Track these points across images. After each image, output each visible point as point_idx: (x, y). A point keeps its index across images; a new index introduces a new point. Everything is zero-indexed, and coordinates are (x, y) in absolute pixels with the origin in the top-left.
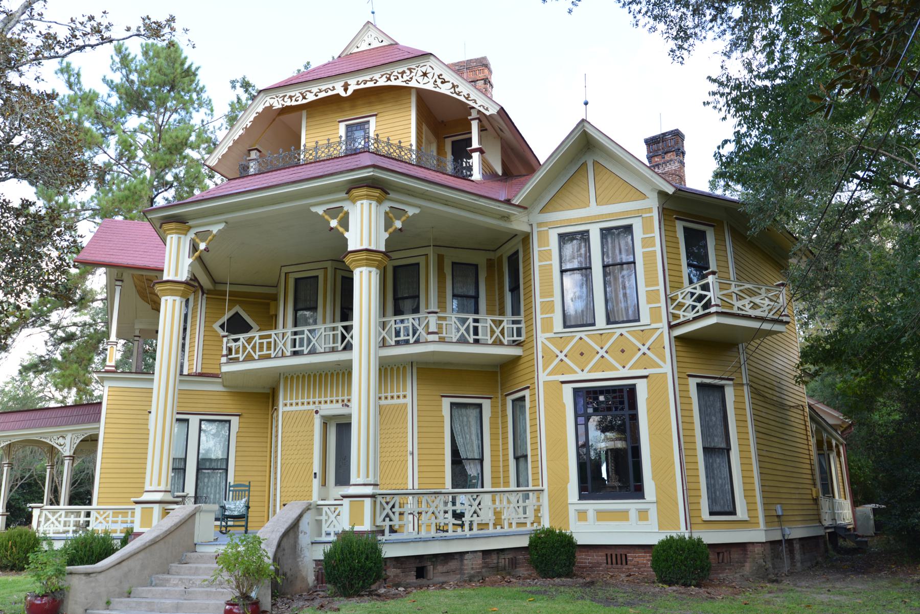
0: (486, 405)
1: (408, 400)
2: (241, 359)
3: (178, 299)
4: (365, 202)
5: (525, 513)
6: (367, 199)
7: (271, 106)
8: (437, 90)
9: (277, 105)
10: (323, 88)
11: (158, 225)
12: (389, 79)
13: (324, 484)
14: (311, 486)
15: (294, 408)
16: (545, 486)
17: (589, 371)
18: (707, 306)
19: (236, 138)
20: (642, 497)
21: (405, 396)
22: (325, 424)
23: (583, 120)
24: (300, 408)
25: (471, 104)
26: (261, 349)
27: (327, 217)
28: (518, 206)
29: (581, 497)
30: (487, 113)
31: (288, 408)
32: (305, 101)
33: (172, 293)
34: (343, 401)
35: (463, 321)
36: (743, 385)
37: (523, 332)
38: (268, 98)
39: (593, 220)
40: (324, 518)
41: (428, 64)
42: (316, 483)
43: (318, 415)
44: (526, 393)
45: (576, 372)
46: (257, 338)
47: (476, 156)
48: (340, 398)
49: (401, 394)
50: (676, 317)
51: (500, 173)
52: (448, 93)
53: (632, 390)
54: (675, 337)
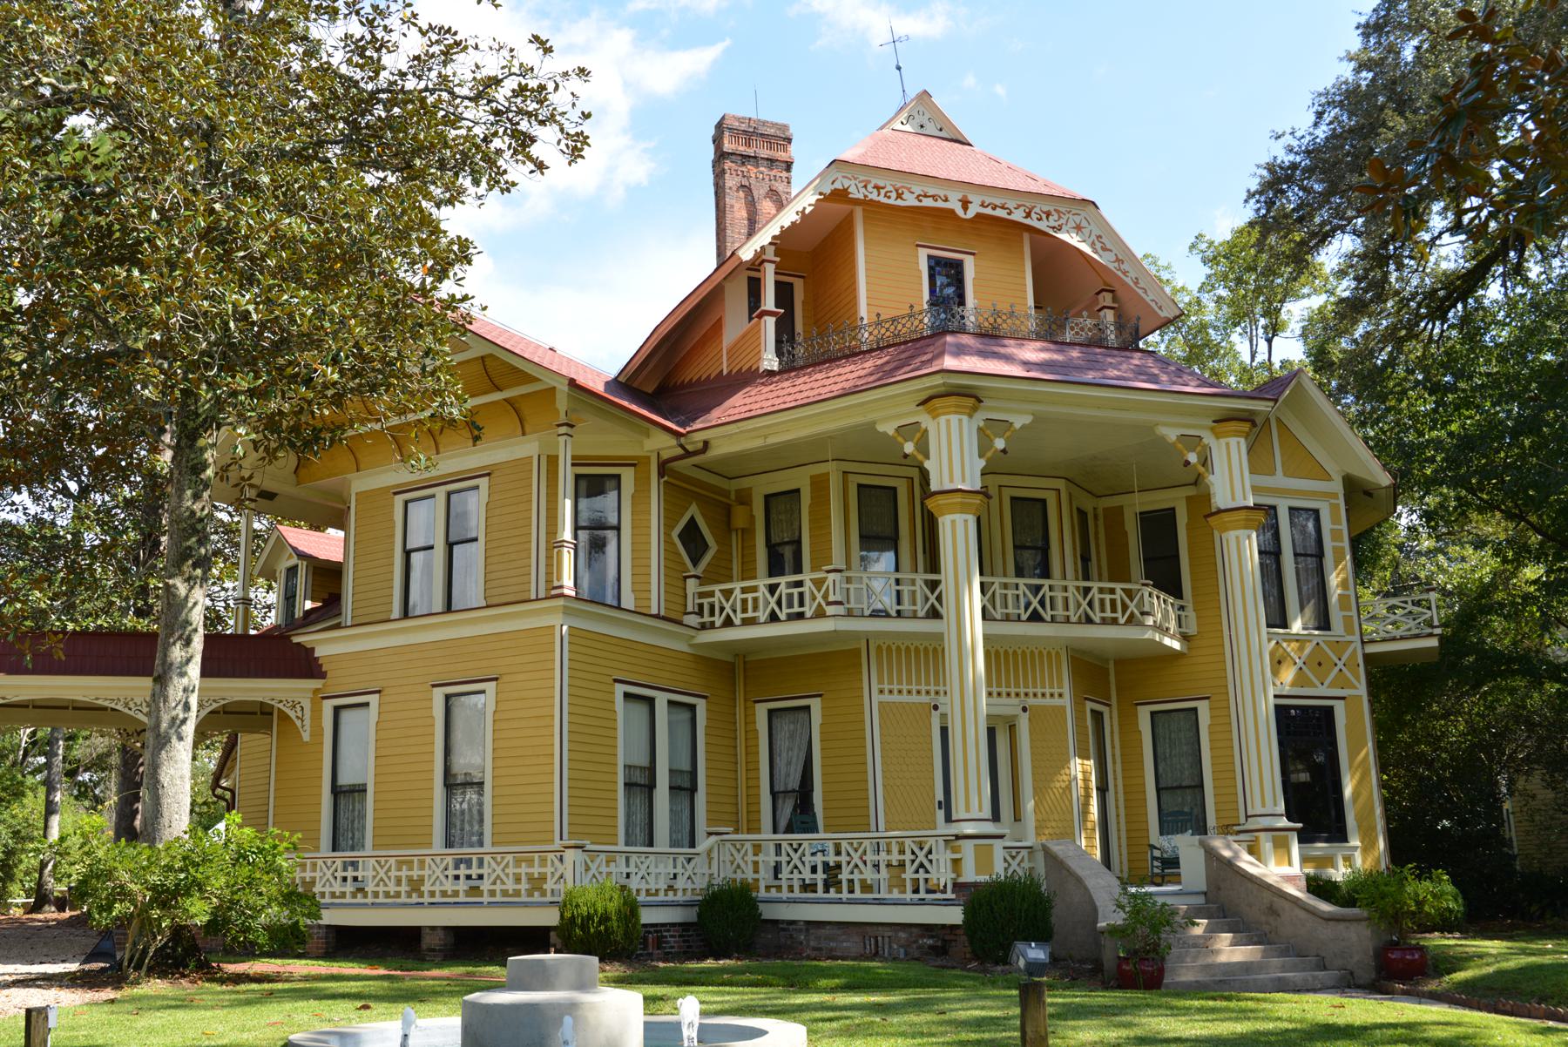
1: (1066, 701)
9: (856, 193)
12: (1028, 215)
15: (895, 698)
19: (787, 224)
20: (1346, 841)
21: (1060, 695)
24: (905, 698)
31: (886, 697)
32: (899, 202)
33: (963, 509)
35: (1087, 590)
38: (839, 175)
43: (935, 715)
49: (1056, 691)
52: (1111, 266)
53: (1329, 711)
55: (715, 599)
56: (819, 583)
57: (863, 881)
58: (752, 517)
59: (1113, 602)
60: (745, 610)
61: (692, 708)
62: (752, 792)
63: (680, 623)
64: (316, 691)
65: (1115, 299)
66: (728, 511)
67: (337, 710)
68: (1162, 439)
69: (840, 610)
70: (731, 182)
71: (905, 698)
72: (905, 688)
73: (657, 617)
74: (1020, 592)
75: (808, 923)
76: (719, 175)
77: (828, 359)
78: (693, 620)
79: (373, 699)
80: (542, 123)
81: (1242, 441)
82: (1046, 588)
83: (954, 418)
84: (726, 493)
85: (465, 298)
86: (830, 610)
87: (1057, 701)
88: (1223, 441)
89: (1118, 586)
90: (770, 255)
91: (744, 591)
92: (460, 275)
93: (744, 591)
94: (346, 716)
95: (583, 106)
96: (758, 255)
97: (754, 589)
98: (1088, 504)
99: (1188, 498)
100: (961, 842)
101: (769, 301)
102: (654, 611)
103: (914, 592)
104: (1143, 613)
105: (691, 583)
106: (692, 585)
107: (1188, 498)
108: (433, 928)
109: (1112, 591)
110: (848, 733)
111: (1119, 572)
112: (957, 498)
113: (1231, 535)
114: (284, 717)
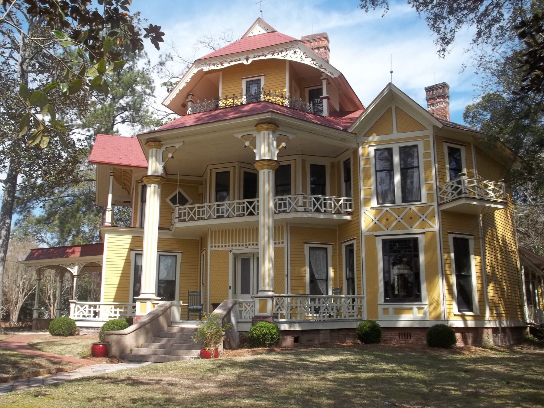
0: (330, 248)
1: (285, 245)
2: (187, 220)
3: (157, 185)
4: (266, 132)
5: (353, 309)
6: (267, 130)
7: (202, 70)
8: (303, 62)
10: (234, 59)
11: (144, 143)
13: (235, 292)
14: (228, 294)
16: (365, 295)
17: (392, 230)
18: (460, 193)
19: (181, 88)
21: (283, 243)
22: (235, 258)
23: (390, 84)
25: (322, 70)
26: (199, 214)
28: (352, 133)
29: (386, 301)
30: (333, 77)
32: (222, 67)
33: (154, 182)
34: (246, 245)
36: (479, 238)
37: (353, 206)
38: (200, 65)
39: (394, 141)
40: (243, 309)
41: (297, 46)
42: (230, 292)
44: (354, 242)
45: (383, 230)
46: (196, 208)
47: (325, 101)
48: (244, 243)
49: (281, 241)
50: (442, 199)
51: (338, 110)
54: (441, 211)
61: (176, 256)
71: (220, 249)
74: (245, 205)
87: (281, 245)
103: (244, 207)
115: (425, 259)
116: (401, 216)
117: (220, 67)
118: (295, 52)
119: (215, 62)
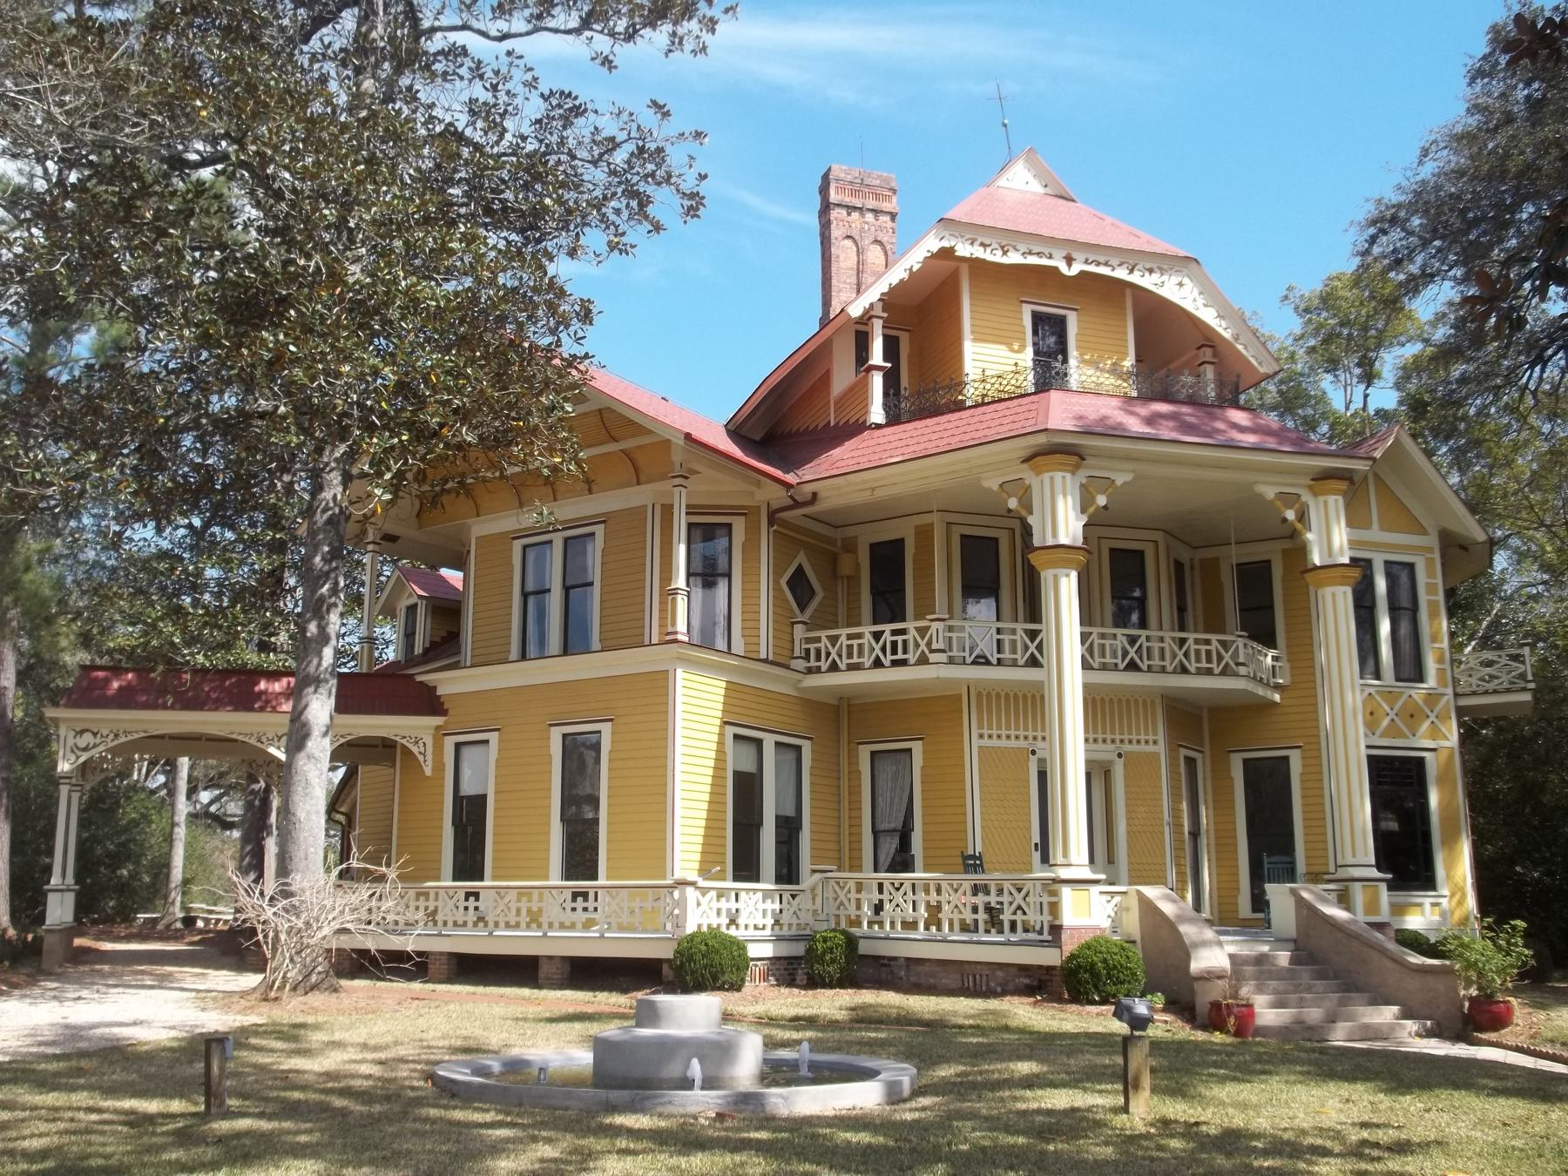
1: (1161, 748)
15: (995, 742)
21: (1155, 742)
27: (1278, 503)
31: (986, 742)
33: (1067, 564)
35: (1182, 641)
38: (946, 233)
49: (1151, 738)
55: (822, 645)
56: (922, 631)
57: (962, 922)
58: (858, 564)
59: (1208, 653)
60: (850, 655)
61: (798, 749)
62: (854, 830)
63: (787, 667)
64: (438, 728)
65: (1215, 355)
66: (834, 559)
67: (458, 746)
68: (1261, 496)
69: (943, 657)
70: (836, 232)
71: (1003, 743)
72: (1004, 733)
73: (766, 661)
75: (908, 959)
76: (825, 226)
77: (936, 412)
78: (800, 664)
79: (493, 737)
80: (659, 184)
81: (1340, 499)
82: (1143, 639)
83: (1058, 475)
84: (832, 542)
85: (586, 356)
86: (933, 657)
87: (1151, 748)
88: (1321, 499)
89: (1214, 638)
90: (878, 311)
91: (850, 637)
92: (580, 334)
93: (850, 637)
94: (466, 752)
95: (699, 167)
96: (866, 312)
97: (859, 636)
98: (1185, 555)
99: (1285, 551)
100: (1056, 886)
101: (877, 356)
102: (763, 656)
104: (1238, 664)
105: (799, 629)
106: (799, 631)
107: (1285, 551)
108: (550, 958)
109: (1208, 642)
110: (947, 775)
111: (1214, 624)
112: (1061, 554)
113: (1327, 592)
114: (407, 752)
115: (1440, 803)
116: (1396, 708)
117: (998, 258)
118: (1180, 284)
119: (987, 242)
